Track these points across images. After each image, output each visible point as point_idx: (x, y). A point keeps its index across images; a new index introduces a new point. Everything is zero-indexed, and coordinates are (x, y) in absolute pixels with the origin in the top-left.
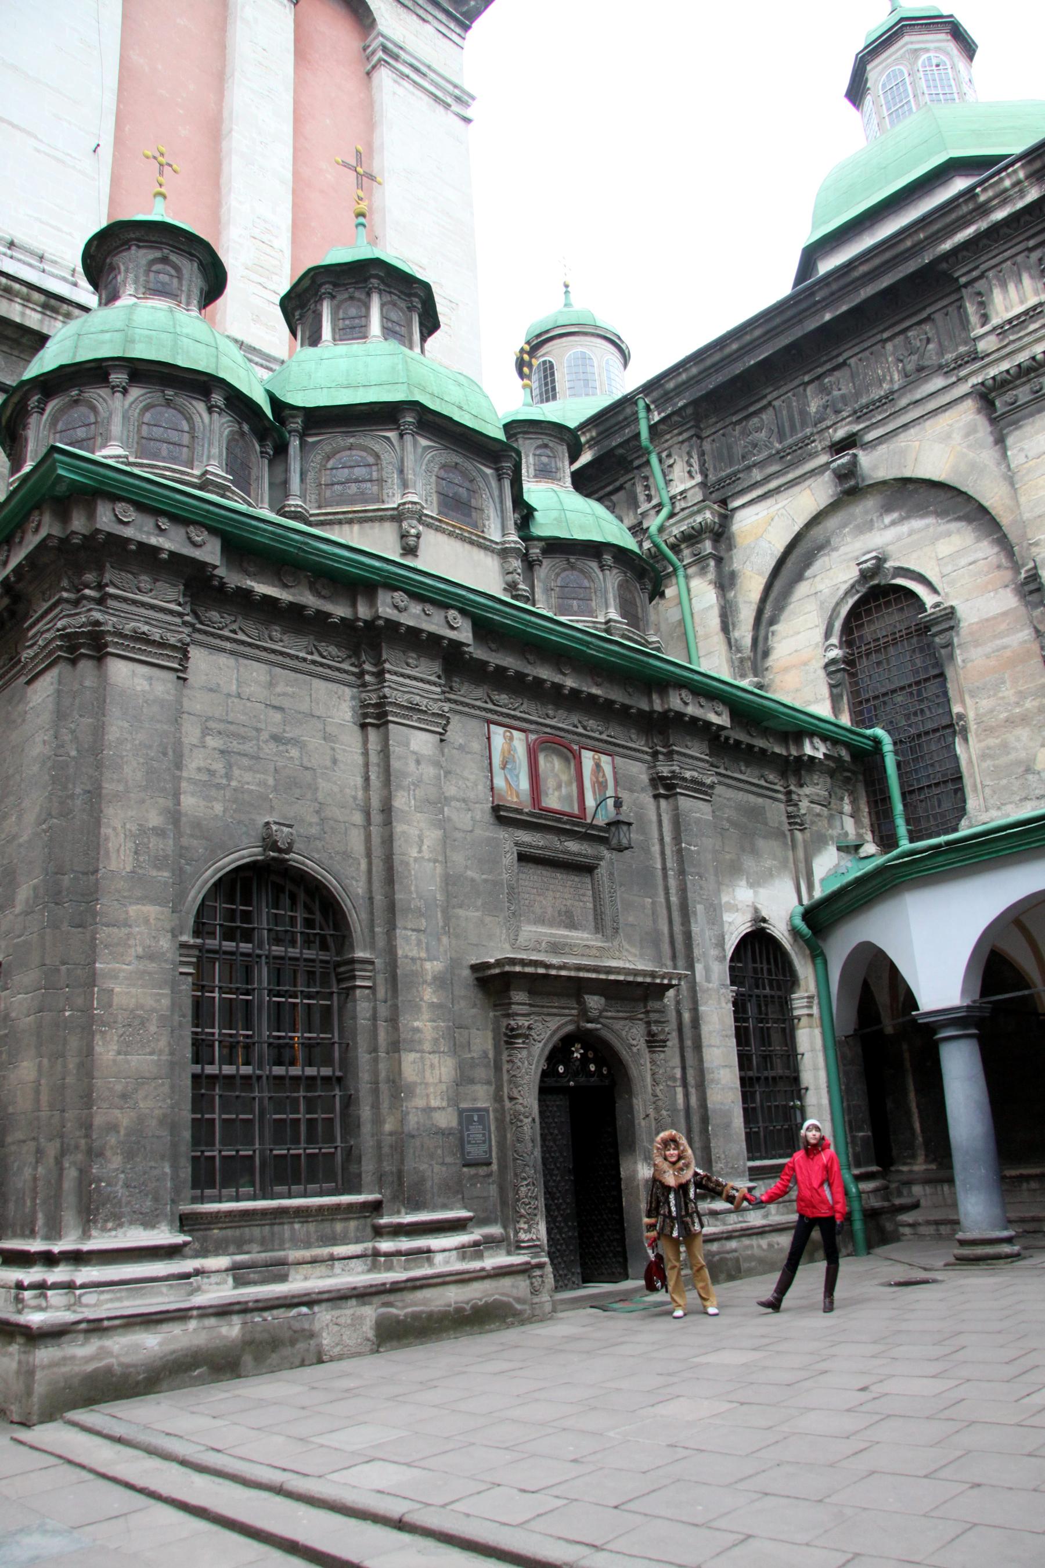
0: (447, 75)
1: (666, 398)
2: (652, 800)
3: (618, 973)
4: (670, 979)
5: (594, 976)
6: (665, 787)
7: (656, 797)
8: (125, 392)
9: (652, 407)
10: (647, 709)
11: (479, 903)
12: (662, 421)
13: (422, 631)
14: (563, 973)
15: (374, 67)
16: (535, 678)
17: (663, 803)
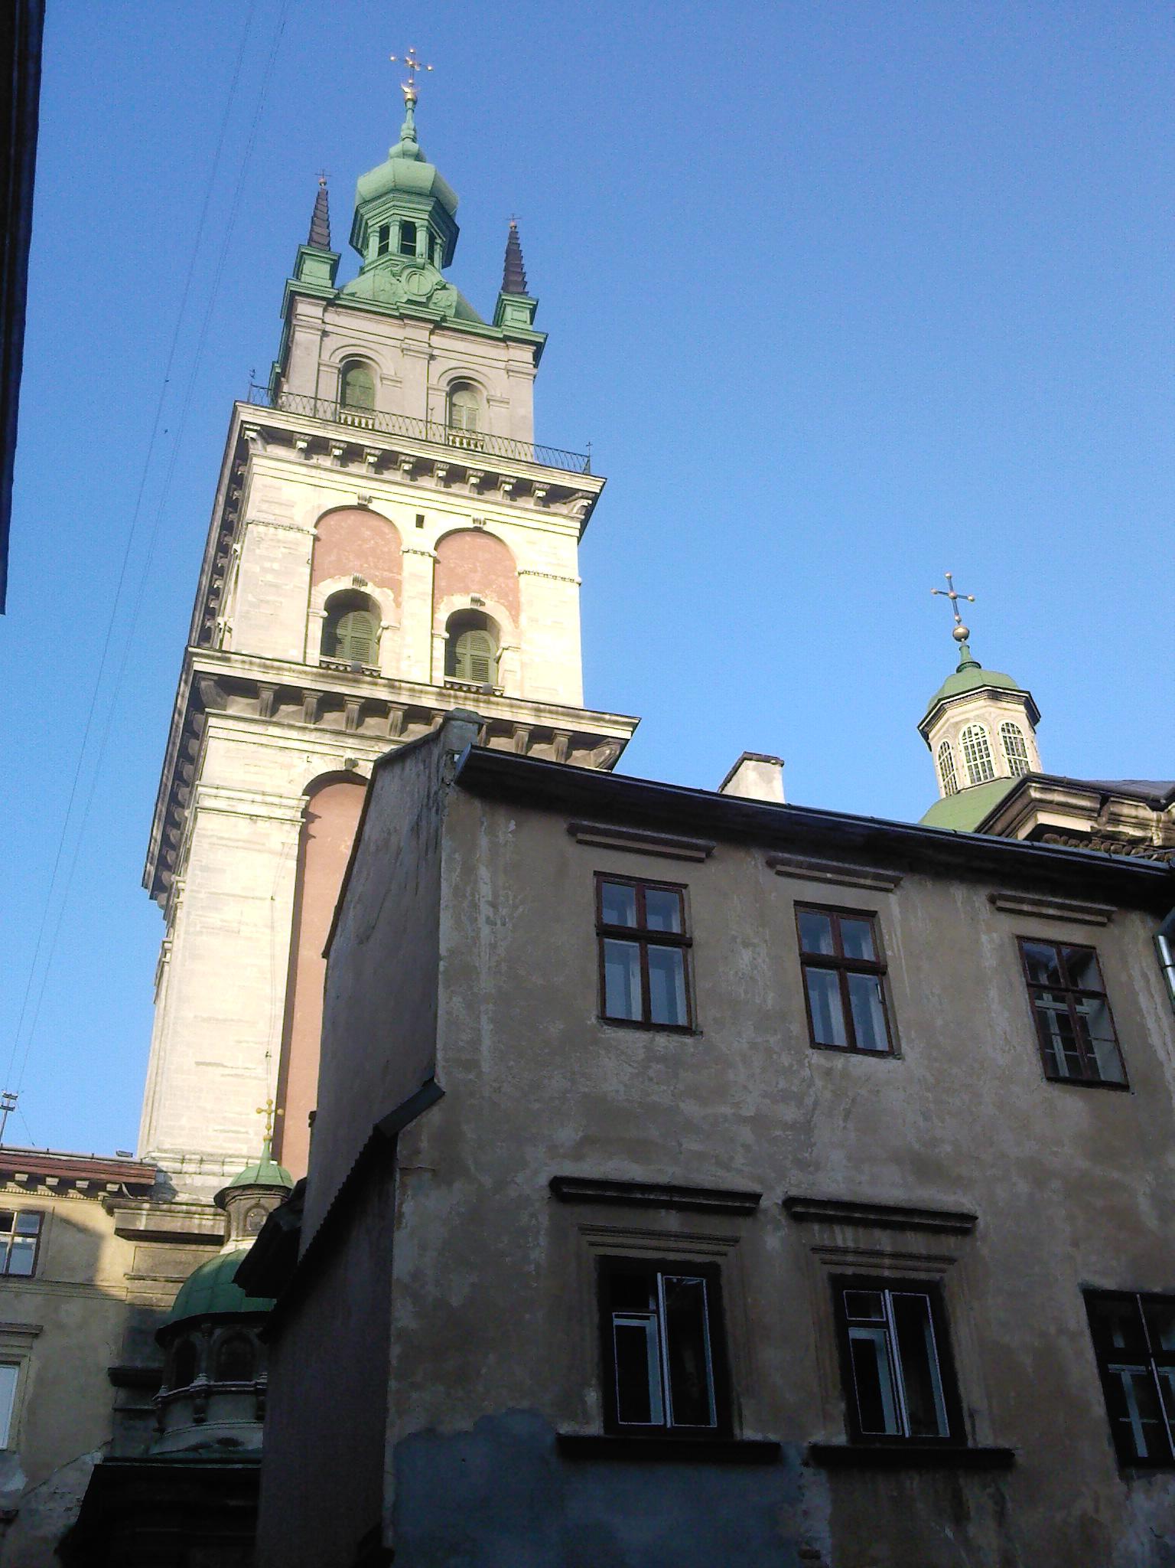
8: (211, 1334)
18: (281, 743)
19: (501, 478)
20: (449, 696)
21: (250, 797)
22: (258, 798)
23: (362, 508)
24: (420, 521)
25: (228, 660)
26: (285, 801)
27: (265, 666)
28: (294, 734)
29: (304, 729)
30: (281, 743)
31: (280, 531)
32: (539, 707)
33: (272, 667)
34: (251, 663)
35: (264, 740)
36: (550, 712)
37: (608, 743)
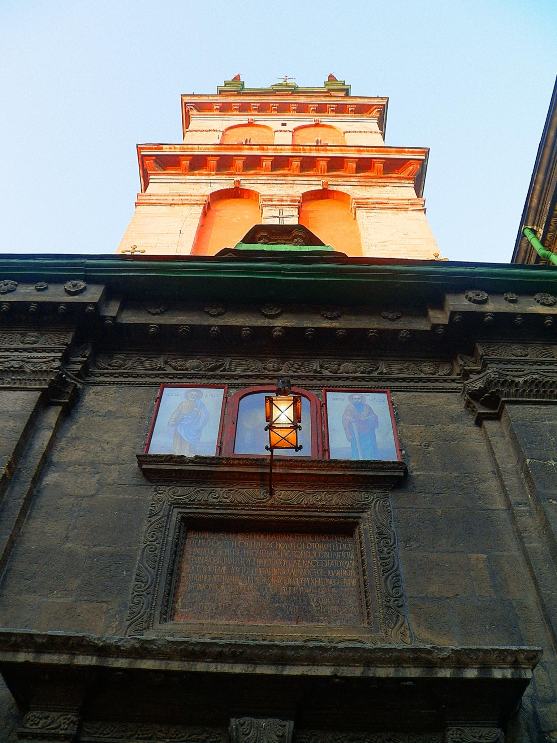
0: (400, 197)
1: (538, 212)
2: (476, 429)
3: (313, 661)
4: (485, 667)
5: (238, 669)
6: (487, 404)
7: (479, 422)
9: (535, 228)
10: (427, 327)
11: (75, 584)
12: (546, 231)
13: (29, 304)
14: (147, 664)
15: (355, 214)
16: (221, 327)
17: (490, 425)
18: (194, 181)
19: (328, 106)
20: (300, 150)
21: (171, 198)
22: (177, 198)
23: (251, 124)
24: (284, 125)
25: (162, 148)
26: (193, 198)
27: (184, 149)
28: (203, 177)
29: (209, 174)
30: (194, 181)
31: (204, 133)
32: (358, 148)
33: (188, 149)
34: (175, 148)
35: (183, 181)
36: (368, 151)
37: (411, 164)
